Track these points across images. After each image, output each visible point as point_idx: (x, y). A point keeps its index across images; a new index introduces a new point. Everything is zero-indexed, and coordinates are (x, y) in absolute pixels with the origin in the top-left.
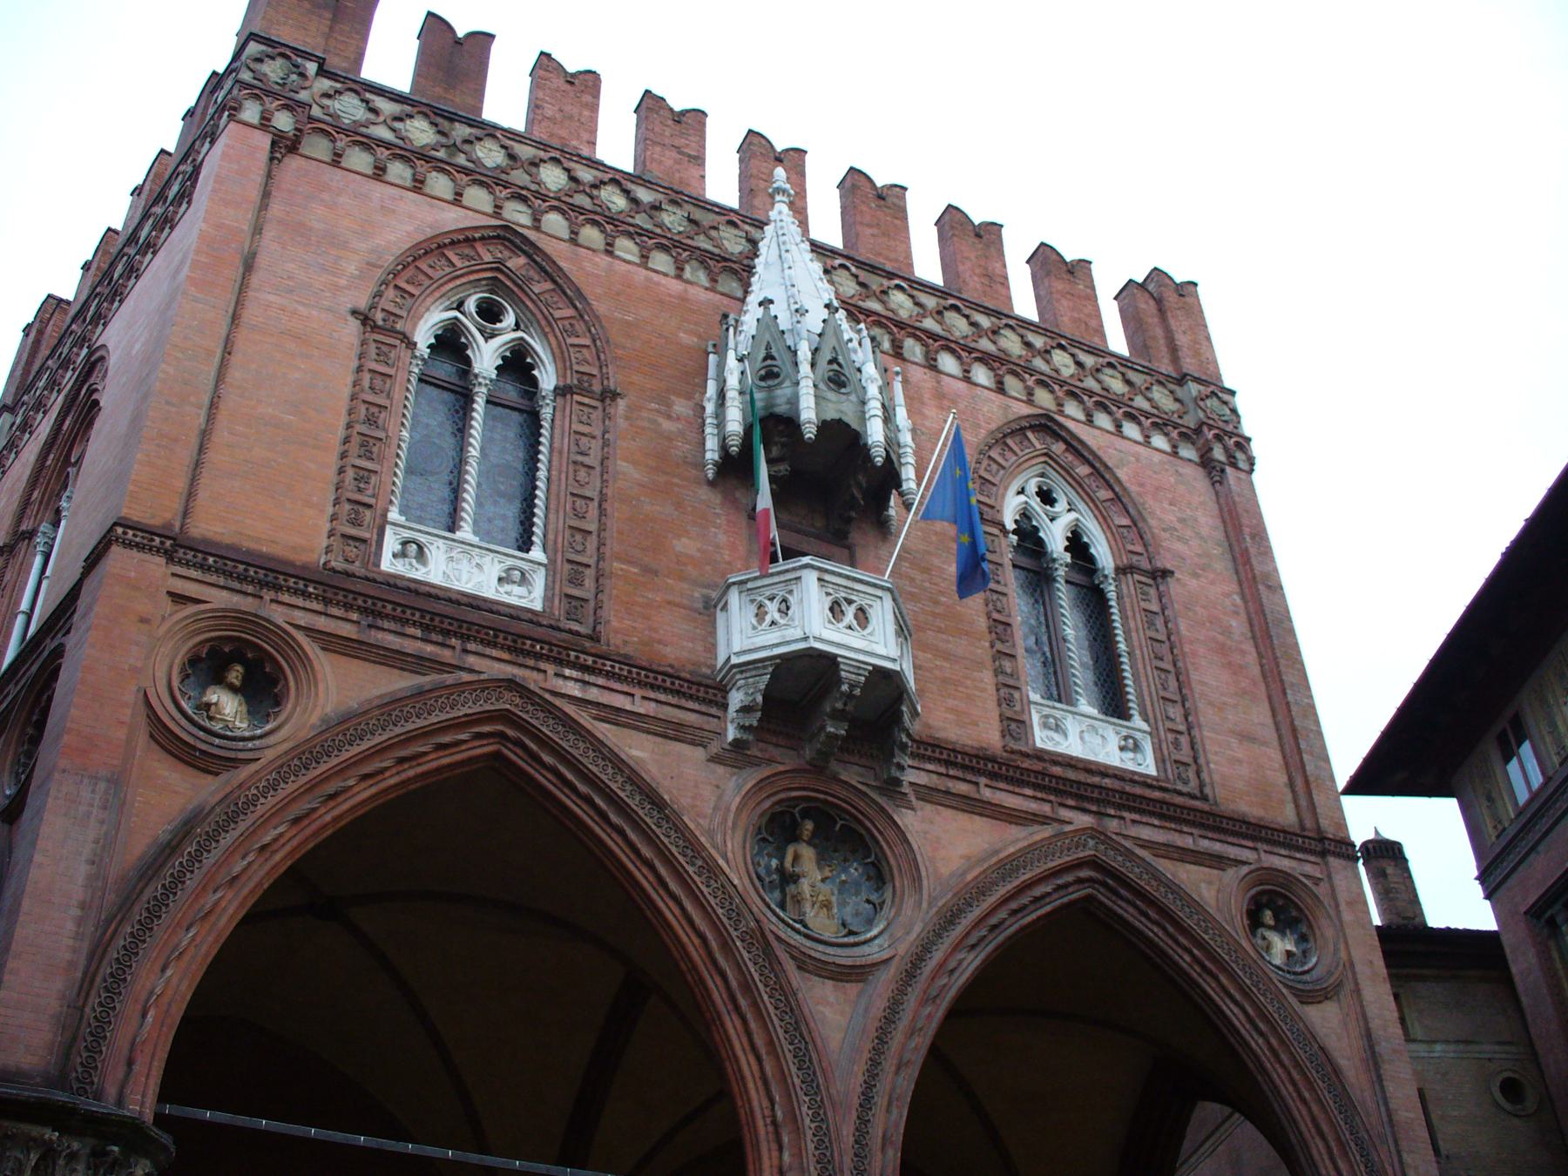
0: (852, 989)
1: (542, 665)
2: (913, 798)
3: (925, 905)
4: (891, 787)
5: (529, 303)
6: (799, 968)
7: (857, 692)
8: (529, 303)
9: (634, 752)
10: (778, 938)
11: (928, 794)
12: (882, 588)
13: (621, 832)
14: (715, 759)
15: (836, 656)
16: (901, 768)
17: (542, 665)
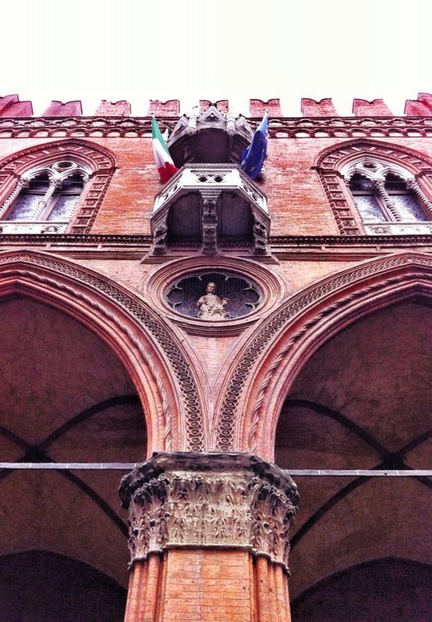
0: (229, 341)
1: (44, 244)
2: (277, 260)
3: (282, 296)
4: (260, 255)
5: (82, 159)
6: (189, 334)
7: (214, 202)
8: (82, 159)
9: (98, 267)
10: (173, 321)
11: (285, 257)
12: (231, 168)
13: (81, 298)
14: (144, 263)
15: (198, 189)
16: (263, 244)
17: (44, 244)
